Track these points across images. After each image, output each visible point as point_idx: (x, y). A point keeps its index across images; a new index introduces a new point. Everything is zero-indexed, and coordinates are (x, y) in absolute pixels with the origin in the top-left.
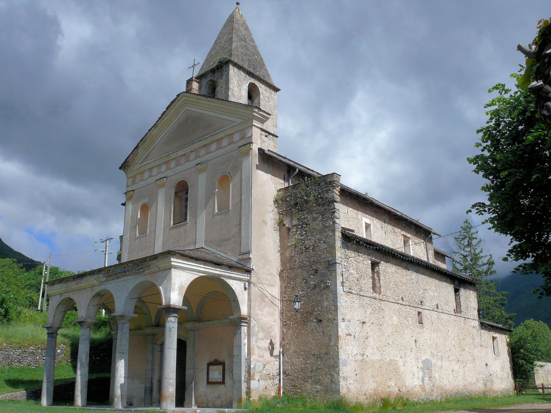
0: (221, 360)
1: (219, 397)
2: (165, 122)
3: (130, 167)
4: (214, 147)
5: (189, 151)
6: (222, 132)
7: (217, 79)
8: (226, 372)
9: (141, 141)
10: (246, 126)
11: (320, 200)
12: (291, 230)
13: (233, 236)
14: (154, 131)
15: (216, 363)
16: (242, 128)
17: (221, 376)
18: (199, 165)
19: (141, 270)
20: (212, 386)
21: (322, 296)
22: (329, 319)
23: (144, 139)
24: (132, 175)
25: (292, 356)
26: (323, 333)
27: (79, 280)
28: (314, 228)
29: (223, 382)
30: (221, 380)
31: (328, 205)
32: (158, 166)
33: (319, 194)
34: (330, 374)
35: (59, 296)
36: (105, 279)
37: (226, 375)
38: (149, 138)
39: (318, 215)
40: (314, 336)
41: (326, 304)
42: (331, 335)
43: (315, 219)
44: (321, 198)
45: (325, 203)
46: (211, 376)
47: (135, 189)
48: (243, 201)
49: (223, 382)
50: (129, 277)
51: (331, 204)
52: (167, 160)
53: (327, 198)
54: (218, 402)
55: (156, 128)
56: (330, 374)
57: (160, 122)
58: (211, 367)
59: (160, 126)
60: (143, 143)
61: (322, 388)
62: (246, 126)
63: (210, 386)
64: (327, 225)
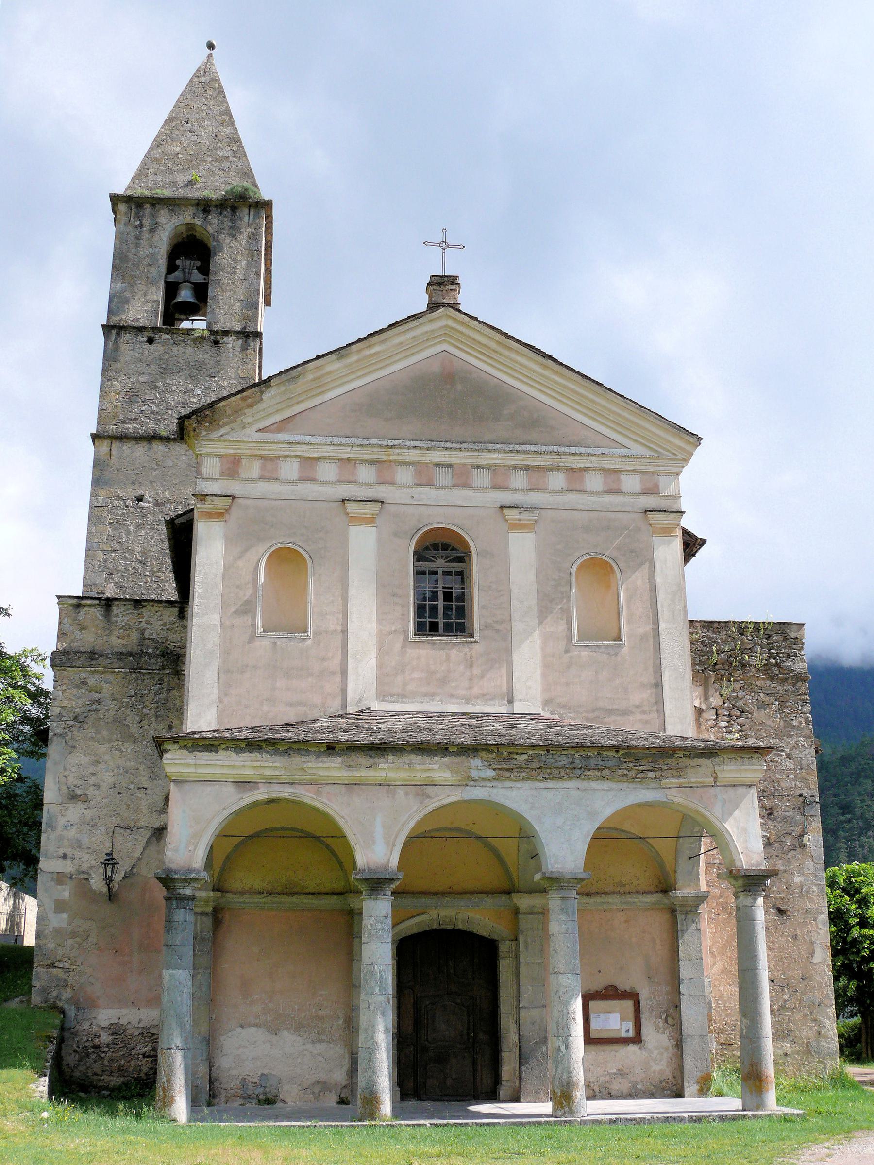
0: (624, 985)
1: (621, 1073)
2: (372, 355)
3: (220, 427)
4: (557, 480)
5: (470, 461)
6: (590, 455)
7: (219, 232)
8: (643, 1017)
9: (281, 373)
10: (661, 468)
11: (775, 670)
12: (705, 715)
13: (638, 707)
14: (333, 365)
15: (611, 993)
16: (651, 469)
17: (630, 1025)
18: (515, 512)
19: (651, 775)
20: (600, 1047)
21: (789, 862)
22: (807, 911)
23: (294, 373)
24: (223, 451)
25: (717, 979)
26: (795, 937)
27: (362, 759)
28: (762, 723)
29: (637, 1039)
30: (631, 1034)
31: (794, 685)
32: (340, 460)
33: (771, 656)
34: (815, 1020)
35: (230, 789)
36: (490, 773)
37: (643, 1022)
38: (310, 377)
39: (772, 699)
40: (773, 942)
41: (798, 879)
42: (812, 943)
43: (763, 706)
44: (777, 665)
45: (787, 679)
46: (594, 1025)
47: (236, 493)
48: (663, 637)
49: (637, 1039)
50: (594, 784)
51: (800, 684)
52: (384, 457)
53: (792, 671)
54: (623, 1085)
55: (342, 357)
56: (815, 1020)
57: (359, 351)
58: (592, 1004)
59: (354, 358)
60: (288, 380)
61: (798, 1047)
62: (661, 468)
63: (592, 1047)
64: (795, 723)
